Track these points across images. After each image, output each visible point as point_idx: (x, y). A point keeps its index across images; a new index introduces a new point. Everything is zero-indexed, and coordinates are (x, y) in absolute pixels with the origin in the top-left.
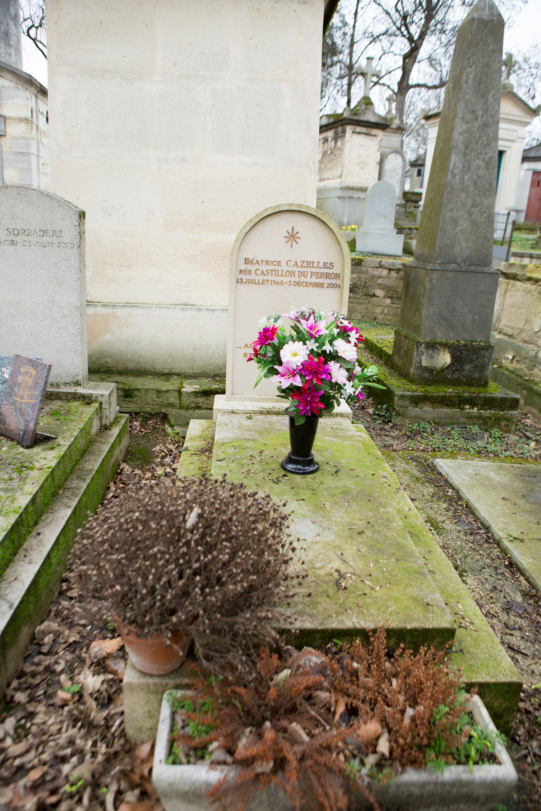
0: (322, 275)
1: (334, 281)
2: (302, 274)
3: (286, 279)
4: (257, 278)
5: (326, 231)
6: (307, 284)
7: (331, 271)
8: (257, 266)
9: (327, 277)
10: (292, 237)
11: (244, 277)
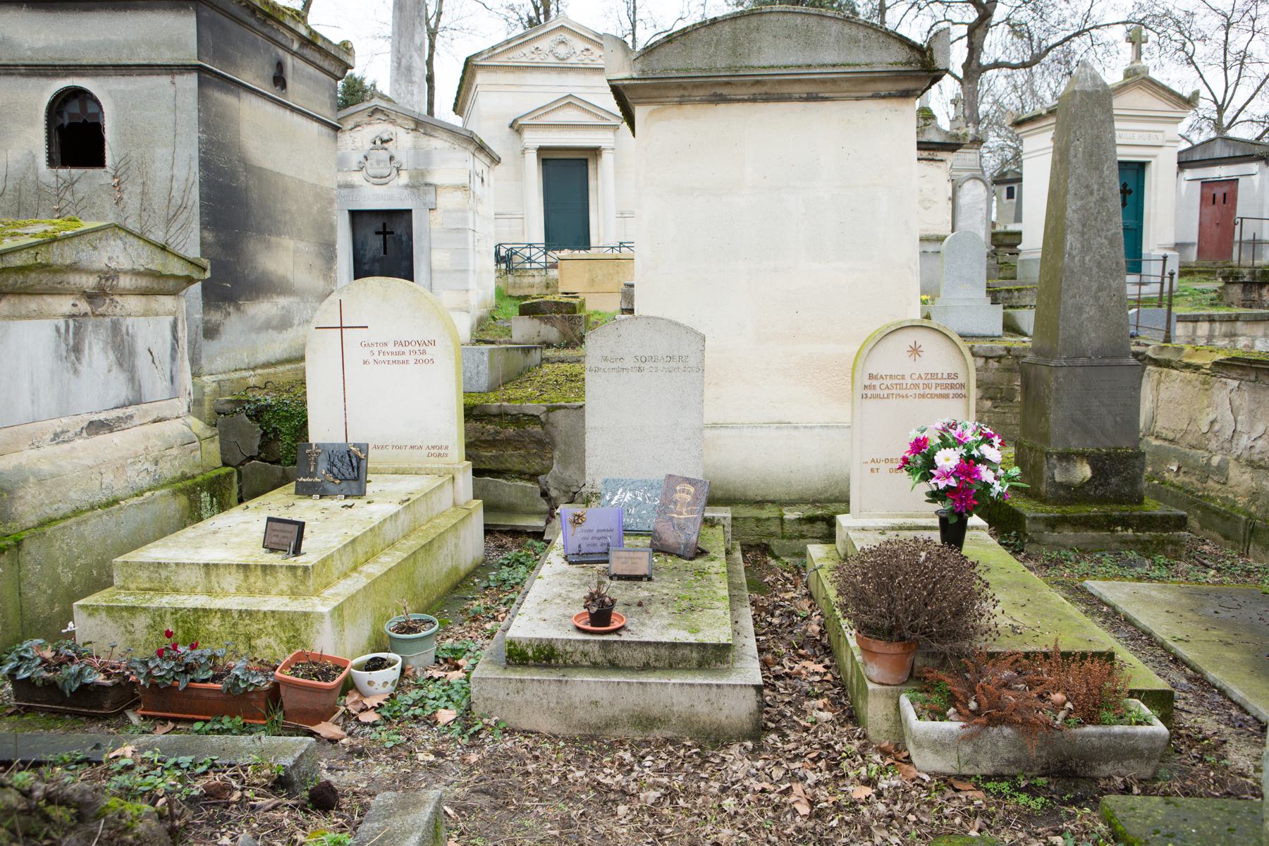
0: (946, 387)
1: (959, 392)
2: (927, 386)
3: (910, 392)
4: (881, 393)
5: (948, 343)
6: (932, 396)
7: (955, 382)
8: (881, 381)
9: (953, 388)
10: (915, 351)
11: (869, 392)
